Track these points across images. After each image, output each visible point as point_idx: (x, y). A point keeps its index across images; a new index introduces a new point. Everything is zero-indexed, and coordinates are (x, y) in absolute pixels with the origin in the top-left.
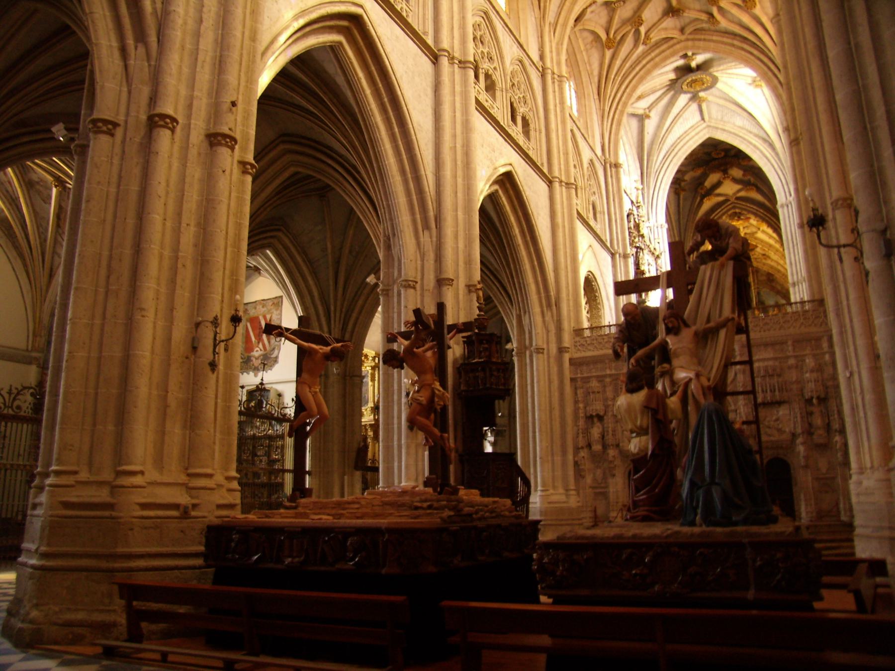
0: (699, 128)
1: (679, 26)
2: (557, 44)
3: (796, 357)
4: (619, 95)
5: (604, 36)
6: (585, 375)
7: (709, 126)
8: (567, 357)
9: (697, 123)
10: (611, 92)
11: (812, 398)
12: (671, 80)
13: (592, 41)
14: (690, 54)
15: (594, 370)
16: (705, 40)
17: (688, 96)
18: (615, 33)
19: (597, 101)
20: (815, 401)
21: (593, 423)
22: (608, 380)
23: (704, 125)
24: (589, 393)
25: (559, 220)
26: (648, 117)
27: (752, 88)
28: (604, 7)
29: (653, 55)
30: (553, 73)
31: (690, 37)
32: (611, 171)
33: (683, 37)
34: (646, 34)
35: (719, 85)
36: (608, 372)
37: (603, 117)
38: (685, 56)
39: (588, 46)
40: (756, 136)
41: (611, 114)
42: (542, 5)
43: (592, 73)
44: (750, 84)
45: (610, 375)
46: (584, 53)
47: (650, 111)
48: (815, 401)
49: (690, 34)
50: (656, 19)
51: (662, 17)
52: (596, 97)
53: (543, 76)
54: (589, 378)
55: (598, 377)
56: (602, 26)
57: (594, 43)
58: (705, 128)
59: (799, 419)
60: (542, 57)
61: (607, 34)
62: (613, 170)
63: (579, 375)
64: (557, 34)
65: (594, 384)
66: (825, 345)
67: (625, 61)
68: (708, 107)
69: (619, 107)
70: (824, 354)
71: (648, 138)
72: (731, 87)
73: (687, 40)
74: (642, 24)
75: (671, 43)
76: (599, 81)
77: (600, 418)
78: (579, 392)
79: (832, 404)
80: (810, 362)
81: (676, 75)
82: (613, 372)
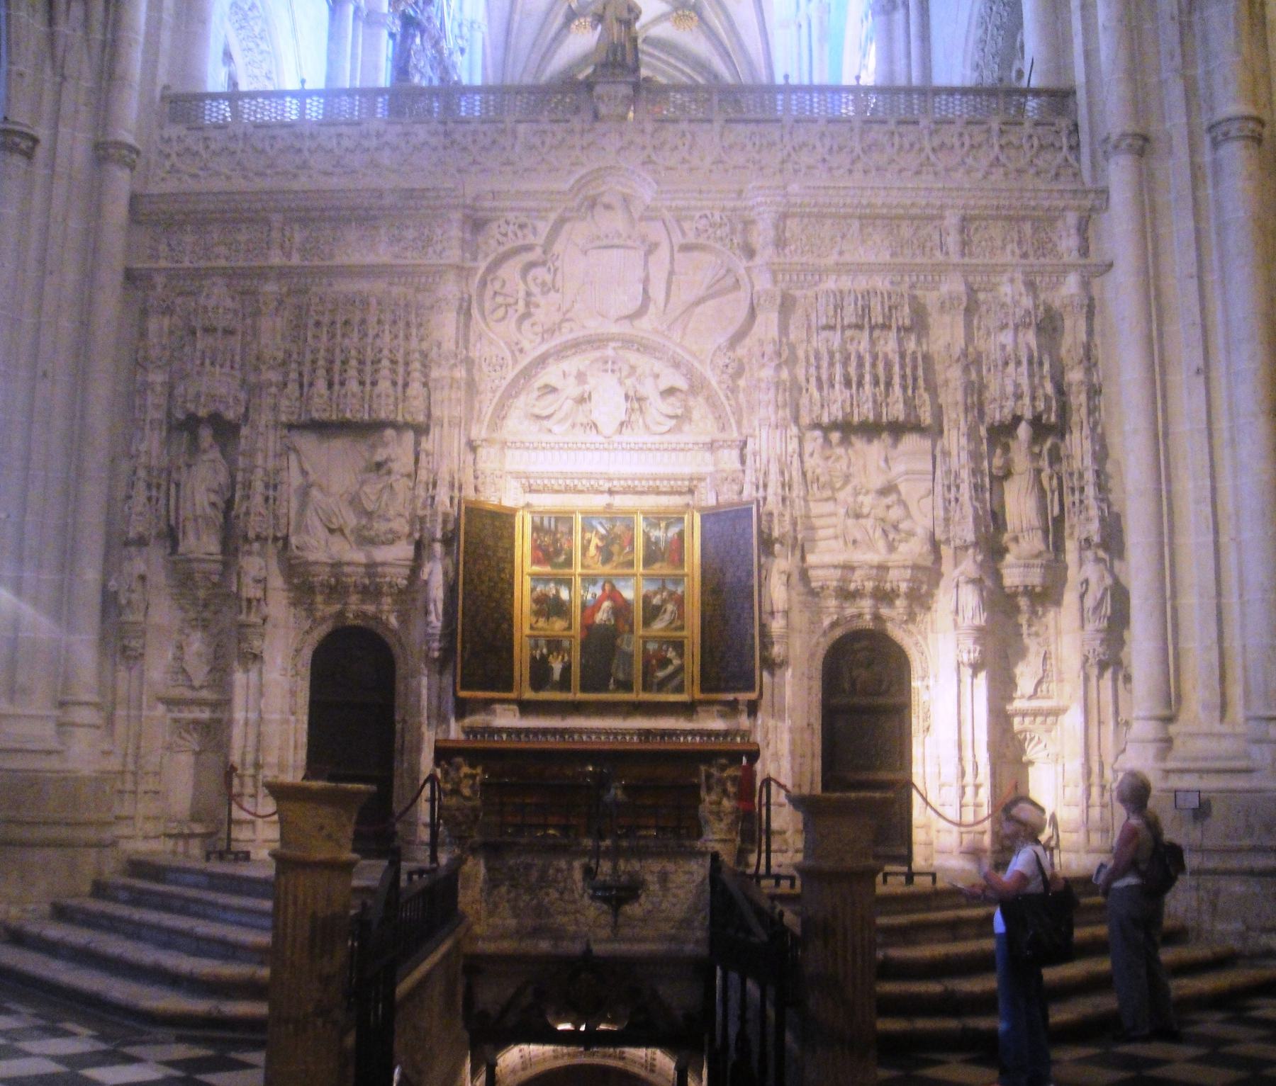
3: (966, 270)
6: (187, 264)
8: (121, 182)
11: (1017, 420)
15: (222, 250)
20: (1023, 431)
21: (194, 448)
22: (271, 288)
24: (194, 333)
36: (276, 259)
45: (283, 273)
48: (1023, 431)
54: (199, 274)
55: (231, 275)
59: (966, 492)
63: (163, 263)
65: (218, 296)
66: (1068, 243)
70: (1065, 269)
77: (226, 431)
78: (153, 324)
79: (1078, 445)
80: (1009, 290)
82: (296, 260)
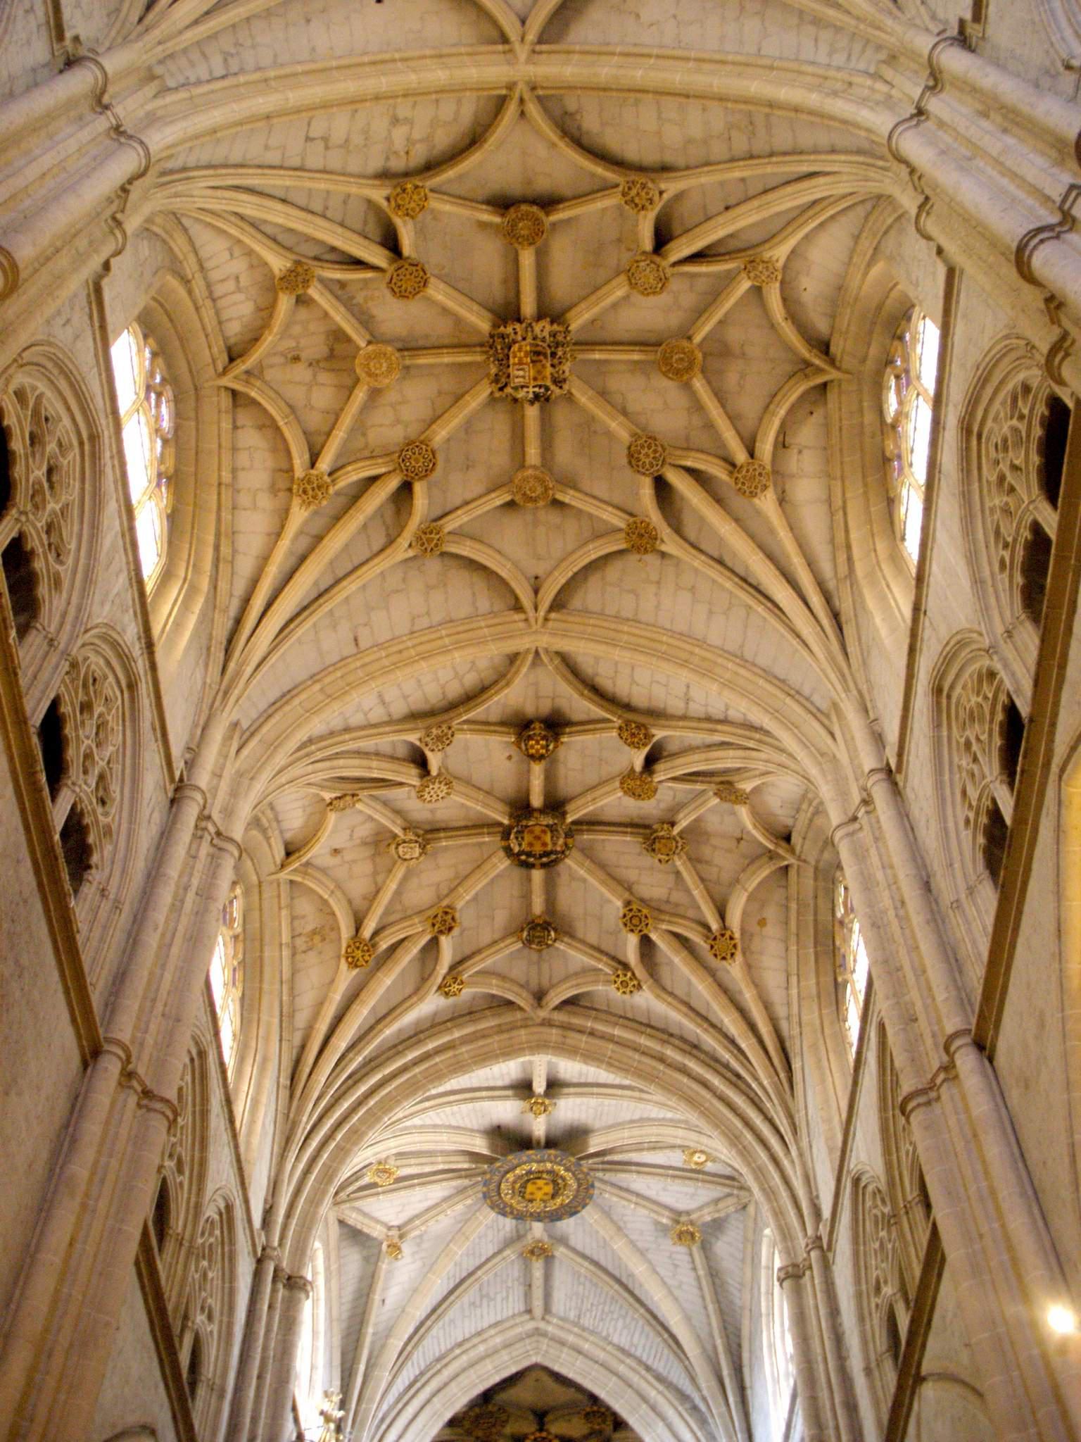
0: (519, 1330)
1: (534, 984)
2: (240, 774)
4: (346, 1105)
5: (346, 932)
7: (538, 1332)
9: (514, 1316)
10: (327, 1085)
12: (474, 1156)
13: (314, 932)
14: (539, 1087)
16: (592, 1033)
17: (508, 1224)
18: (376, 933)
19: (284, 1094)
23: (530, 1326)
25: (80, 1169)
26: (395, 1248)
27: (668, 1245)
28: (368, 852)
29: (457, 1034)
30: (204, 817)
31: (560, 1017)
32: (274, 1291)
33: (543, 1014)
34: (452, 968)
35: (589, 1214)
37: (288, 1140)
38: (523, 1088)
39: (300, 942)
40: (660, 1378)
41: (314, 1144)
42: (232, 665)
43: (292, 1016)
44: (664, 1230)
46: (286, 953)
47: (401, 1237)
49: (557, 1008)
50: (486, 938)
51: (503, 939)
52: (285, 1081)
53: (176, 800)
56: (350, 902)
57: (317, 938)
58: (529, 1336)
60: (190, 765)
61: (357, 930)
62: (281, 1292)
64: (245, 752)
67: (381, 1020)
68: (548, 1278)
69: (339, 1136)
71: (378, 1317)
72: (619, 1229)
73: (547, 1023)
74: (450, 929)
75: (508, 1017)
76: (303, 1047)
81: (493, 1147)
